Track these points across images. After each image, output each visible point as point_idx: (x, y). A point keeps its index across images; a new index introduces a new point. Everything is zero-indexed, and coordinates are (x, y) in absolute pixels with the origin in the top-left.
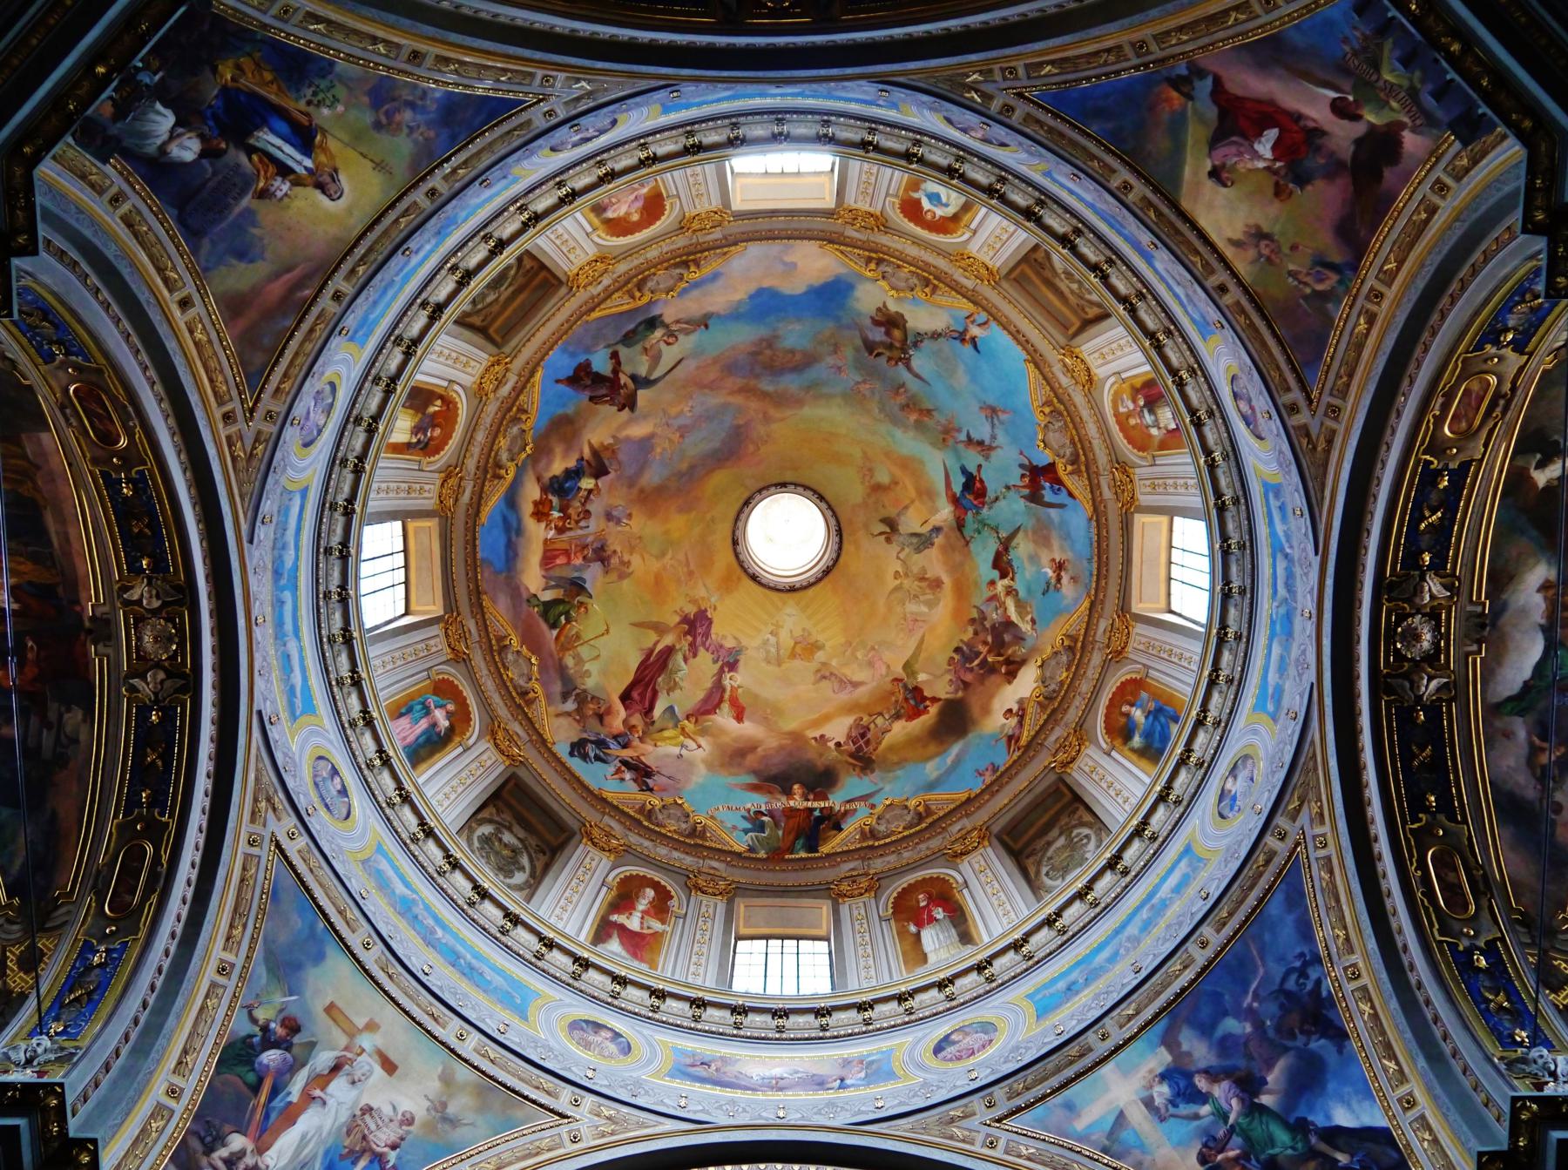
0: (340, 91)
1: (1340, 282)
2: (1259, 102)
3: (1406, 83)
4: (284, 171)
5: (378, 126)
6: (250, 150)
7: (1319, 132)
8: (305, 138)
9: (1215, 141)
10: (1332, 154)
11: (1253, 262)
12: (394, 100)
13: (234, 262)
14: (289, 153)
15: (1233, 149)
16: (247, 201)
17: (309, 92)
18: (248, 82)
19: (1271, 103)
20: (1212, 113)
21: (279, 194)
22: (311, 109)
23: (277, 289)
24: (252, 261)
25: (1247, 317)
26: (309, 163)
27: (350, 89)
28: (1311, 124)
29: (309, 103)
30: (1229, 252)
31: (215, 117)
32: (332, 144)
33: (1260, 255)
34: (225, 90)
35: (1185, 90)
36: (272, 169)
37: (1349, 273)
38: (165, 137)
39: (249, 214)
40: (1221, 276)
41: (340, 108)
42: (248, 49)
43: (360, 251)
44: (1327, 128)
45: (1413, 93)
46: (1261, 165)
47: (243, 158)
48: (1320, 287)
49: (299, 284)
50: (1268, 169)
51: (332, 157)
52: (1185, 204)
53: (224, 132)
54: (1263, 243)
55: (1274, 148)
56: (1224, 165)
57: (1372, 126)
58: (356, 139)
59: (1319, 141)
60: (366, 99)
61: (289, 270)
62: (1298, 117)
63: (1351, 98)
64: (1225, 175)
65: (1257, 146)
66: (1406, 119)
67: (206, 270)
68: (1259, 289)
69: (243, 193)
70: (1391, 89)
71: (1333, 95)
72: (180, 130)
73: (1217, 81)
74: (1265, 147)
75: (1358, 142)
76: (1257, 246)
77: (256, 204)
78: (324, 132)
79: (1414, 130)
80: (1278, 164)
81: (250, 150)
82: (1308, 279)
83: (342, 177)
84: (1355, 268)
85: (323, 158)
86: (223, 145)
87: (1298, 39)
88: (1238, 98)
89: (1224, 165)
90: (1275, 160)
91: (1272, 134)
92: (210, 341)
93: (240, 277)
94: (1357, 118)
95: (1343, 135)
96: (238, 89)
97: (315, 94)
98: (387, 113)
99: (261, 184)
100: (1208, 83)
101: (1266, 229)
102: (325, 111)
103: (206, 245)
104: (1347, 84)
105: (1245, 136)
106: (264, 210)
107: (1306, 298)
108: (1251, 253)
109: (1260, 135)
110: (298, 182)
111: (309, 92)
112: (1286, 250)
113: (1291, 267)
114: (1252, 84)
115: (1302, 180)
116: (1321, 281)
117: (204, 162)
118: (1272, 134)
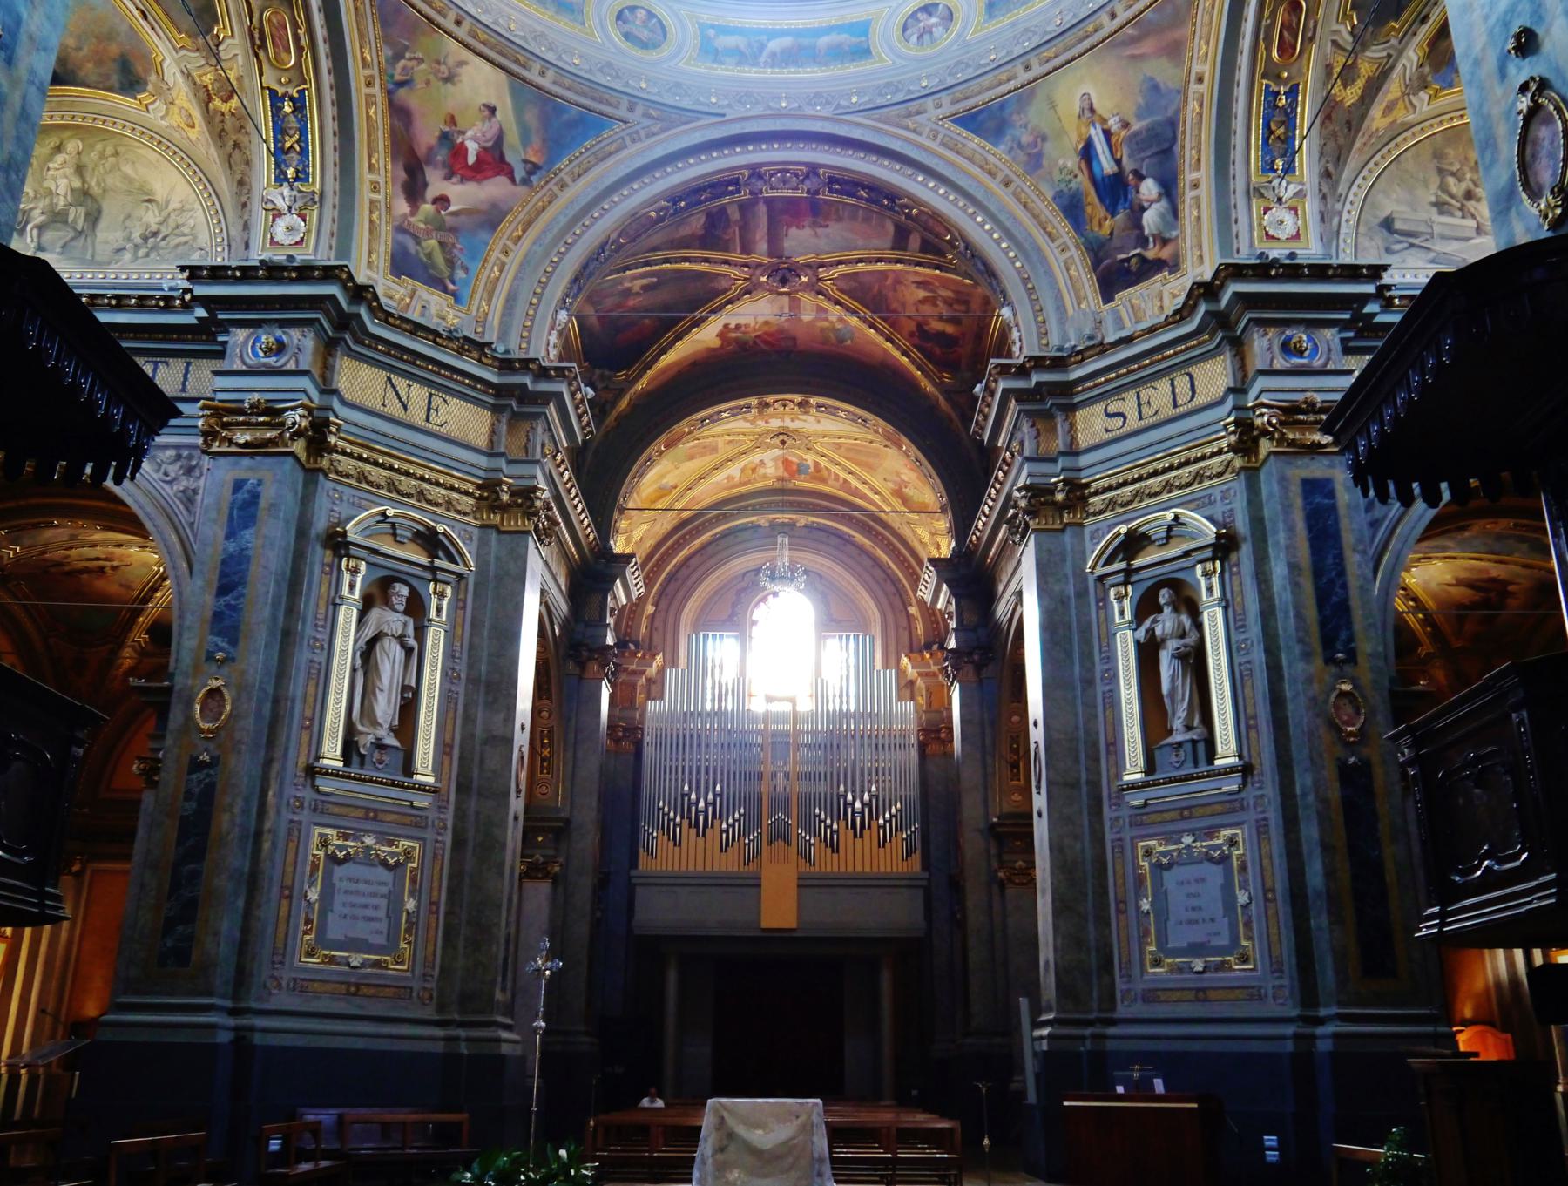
0: (1057, 176)
1: (392, 76)
2: (486, 178)
3: (424, 244)
4: (1107, 134)
5: (1044, 139)
6: (1118, 162)
7: (448, 177)
8: (1087, 153)
9: (499, 139)
10: (435, 167)
11: (446, 57)
12: (1029, 155)
13: (1162, 86)
14: (1100, 146)
15: (489, 135)
16: (1136, 126)
17: (1072, 185)
18: (1101, 211)
19: (479, 181)
20: (510, 157)
21: (1117, 118)
22: (1077, 171)
23: (1146, 47)
24: (1152, 79)
25: (435, 9)
26: (1092, 131)
27: (1050, 173)
28: (454, 179)
29: (1076, 176)
30: (466, 54)
31: (1126, 199)
32: (1074, 137)
33: (445, 63)
34: (1113, 215)
35: (529, 166)
36: (1114, 139)
37: (391, 86)
38: (1155, 206)
39: (1139, 117)
40: (461, 32)
41: (1061, 162)
42: (1091, 235)
43: (1086, 44)
44: (446, 183)
45: (418, 241)
46: (469, 133)
47: (1125, 160)
48: (402, 63)
49: (1134, 41)
50: (463, 133)
51: (1078, 128)
52: (503, 76)
53: (1126, 185)
54: (446, 75)
55: (466, 150)
56: (490, 120)
57: (425, 202)
58: (1062, 132)
59: (445, 171)
60: (1045, 162)
61: (1133, 57)
62: (464, 179)
63: (443, 213)
64: (487, 113)
65: (476, 146)
66: (412, 219)
67: (1179, 92)
68: (436, 35)
69: (1136, 134)
70: (428, 234)
71: (452, 208)
72: (1146, 204)
73: (513, 180)
74: (472, 149)
75: (426, 185)
76: (449, 69)
77: (1132, 121)
78: (1076, 150)
79: (405, 216)
80: (459, 140)
81: (1118, 162)
82: (410, 64)
83: (1077, 110)
84: (390, 93)
85: (1083, 130)
86: (1131, 177)
87: (483, 235)
88: (498, 174)
89: (490, 120)
90: (462, 143)
91: (471, 159)
92: (1201, 38)
93: (1162, 71)
94: (435, 201)
95: (437, 184)
96: (1107, 210)
97: (1070, 181)
98: (1036, 146)
99: (1124, 132)
100: (518, 177)
101: (449, 85)
102: (1069, 164)
103: (1170, 112)
104: (449, 221)
105: (485, 149)
106: (1129, 114)
107: (406, 48)
108: (451, 61)
109: (478, 156)
110: (1104, 121)
111: (1073, 185)
112: (431, 77)
113: (423, 66)
114: (494, 189)
115: (445, 137)
116: (404, 68)
117: (1144, 172)
118: (471, 159)
